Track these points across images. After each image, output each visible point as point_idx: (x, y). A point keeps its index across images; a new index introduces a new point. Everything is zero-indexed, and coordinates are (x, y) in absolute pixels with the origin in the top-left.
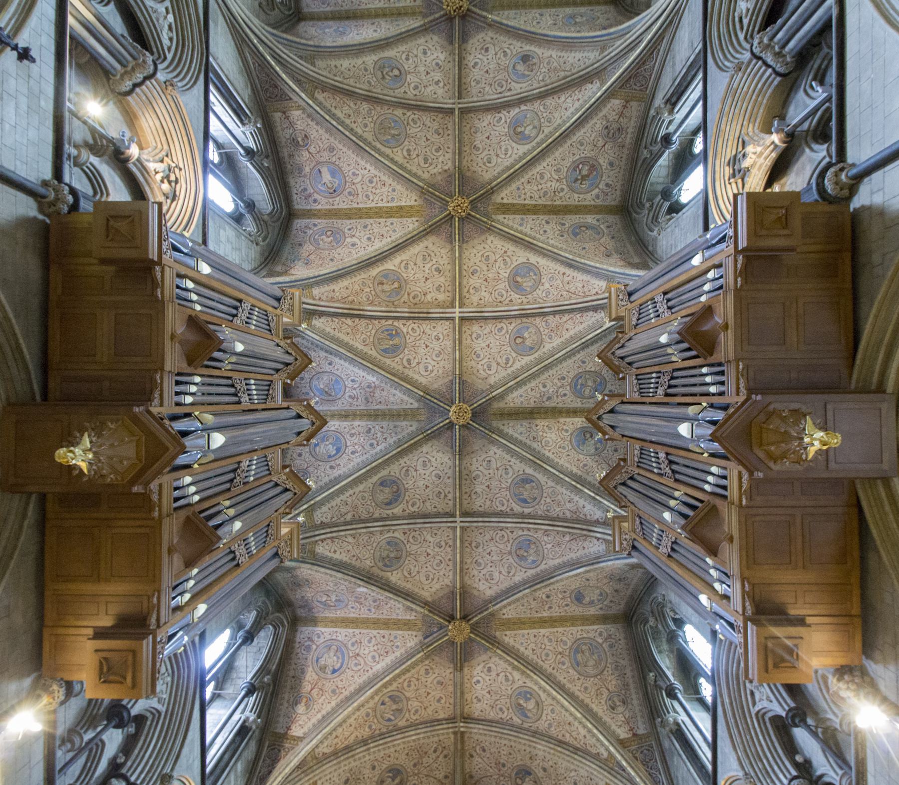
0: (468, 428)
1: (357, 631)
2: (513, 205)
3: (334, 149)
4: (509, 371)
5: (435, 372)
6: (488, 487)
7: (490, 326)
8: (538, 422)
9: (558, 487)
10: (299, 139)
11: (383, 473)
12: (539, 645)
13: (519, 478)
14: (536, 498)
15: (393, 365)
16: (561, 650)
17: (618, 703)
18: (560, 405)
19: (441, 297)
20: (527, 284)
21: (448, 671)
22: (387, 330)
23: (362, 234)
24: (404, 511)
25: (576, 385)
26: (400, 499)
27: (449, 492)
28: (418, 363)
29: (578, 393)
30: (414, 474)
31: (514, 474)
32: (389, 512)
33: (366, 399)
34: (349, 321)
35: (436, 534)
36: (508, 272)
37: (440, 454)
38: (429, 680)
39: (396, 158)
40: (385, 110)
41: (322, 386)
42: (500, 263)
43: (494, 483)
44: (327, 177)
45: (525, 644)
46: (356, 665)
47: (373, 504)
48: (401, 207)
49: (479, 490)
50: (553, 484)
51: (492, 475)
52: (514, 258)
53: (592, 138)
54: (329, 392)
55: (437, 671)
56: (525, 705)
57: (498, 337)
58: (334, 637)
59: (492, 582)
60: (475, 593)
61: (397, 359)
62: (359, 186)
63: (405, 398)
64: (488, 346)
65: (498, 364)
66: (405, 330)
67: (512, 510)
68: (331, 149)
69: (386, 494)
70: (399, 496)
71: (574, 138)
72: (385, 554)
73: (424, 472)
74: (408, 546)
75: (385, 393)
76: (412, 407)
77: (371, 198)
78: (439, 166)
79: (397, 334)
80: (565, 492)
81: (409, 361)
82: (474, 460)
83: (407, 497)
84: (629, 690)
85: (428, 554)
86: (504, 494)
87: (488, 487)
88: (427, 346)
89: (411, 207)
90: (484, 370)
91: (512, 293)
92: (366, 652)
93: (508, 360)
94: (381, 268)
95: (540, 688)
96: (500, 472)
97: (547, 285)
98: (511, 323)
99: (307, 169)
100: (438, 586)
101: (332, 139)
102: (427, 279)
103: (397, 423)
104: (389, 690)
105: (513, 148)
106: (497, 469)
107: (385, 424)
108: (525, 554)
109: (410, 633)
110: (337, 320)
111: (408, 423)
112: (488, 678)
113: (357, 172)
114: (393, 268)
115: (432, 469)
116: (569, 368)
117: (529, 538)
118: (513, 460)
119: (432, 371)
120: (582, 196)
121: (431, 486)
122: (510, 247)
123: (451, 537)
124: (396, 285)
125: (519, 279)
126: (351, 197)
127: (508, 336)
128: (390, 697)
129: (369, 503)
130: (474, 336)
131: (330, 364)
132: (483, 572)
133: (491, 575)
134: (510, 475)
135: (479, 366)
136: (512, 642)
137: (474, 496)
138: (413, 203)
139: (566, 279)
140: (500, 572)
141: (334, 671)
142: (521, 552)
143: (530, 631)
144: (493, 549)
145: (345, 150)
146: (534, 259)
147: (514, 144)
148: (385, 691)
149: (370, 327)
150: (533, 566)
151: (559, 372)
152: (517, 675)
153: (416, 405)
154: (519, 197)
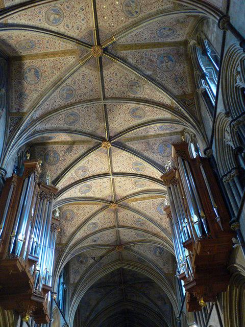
4: (87, 159)
18: (62, 146)
25: (57, 157)
29: (55, 152)
40: (141, 227)
41: (168, 149)
49: (94, 114)
55: (107, 25)
56: (55, 16)
60: (90, 68)
69: (139, 113)
86: (82, 115)
93: (88, 163)
104: (134, 19)
107: (140, 135)
117: (67, 100)
118: (80, 128)
122: (93, 196)
128: (133, 15)
133: (83, 77)
136: (68, 45)
143: (58, 50)
146: (83, 195)
153: (126, 144)
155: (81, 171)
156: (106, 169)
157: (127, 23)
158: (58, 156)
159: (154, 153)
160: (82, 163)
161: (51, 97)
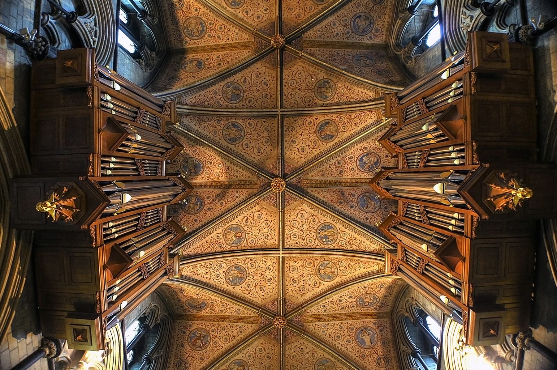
0: (273, 174)
1: (346, 40)
2: (244, 322)
3: (362, 357)
4: (245, 214)
5: (296, 213)
6: (259, 135)
7: (259, 244)
8: (226, 179)
9: (212, 136)
10: (383, 362)
11: (331, 144)
12: (226, 34)
13: (238, 142)
14: (227, 128)
15: (324, 218)
16: (212, 32)
17: (177, 4)
18: (211, 190)
19: (292, 263)
20: (234, 272)
21: (285, 16)
22: (329, 241)
23: (345, 304)
24: (317, 119)
25: (201, 205)
26: (319, 126)
27: (286, 131)
28: (308, 219)
29: (199, 199)
30: (310, 143)
31: (242, 144)
32: (326, 118)
33: (343, 194)
34: (354, 248)
35: (295, 103)
36: (247, 281)
37: (292, 157)
38: (297, 10)
39: (321, 351)
41: (373, 202)
42: (253, 286)
43: (255, 137)
44: (367, 339)
45: (235, 34)
46: (346, 20)
47: (337, 123)
48: (319, 321)
49: (265, 132)
50: (215, 138)
51: (257, 143)
52: (243, 289)
53: (195, 362)
54: (368, 199)
55: (293, 16)
57: (253, 236)
58: (361, 37)
59: (256, 72)
60: (267, 65)
61: (322, 222)
62: (346, 334)
63: (316, 195)
64: (260, 231)
65: (253, 219)
66: (317, 241)
67: (243, 120)
68: (363, 356)
69: (329, 130)
70: (320, 129)
71: (206, 362)
72: (329, 90)
73: (303, 145)
74: (313, 95)
75: (330, 198)
76: (312, 189)
77: (338, 326)
78: (293, 347)
79: (322, 238)
80: (208, 134)
81: (314, 220)
82: (269, 153)
83: (315, 128)
84: (170, 12)
85: (300, 89)
87: (259, 135)
88: (302, 230)
89: (312, 321)
90: (262, 214)
91: (244, 266)
92: (339, 28)
93: (247, 222)
94: (332, 282)
95: (225, 9)
96: (251, 145)
97: (221, 271)
98: (245, 246)
99: (379, 344)
100: (293, 69)
101: (362, 362)
102: (302, 275)
103: (322, 178)
104: (324, 5)
105: (245, 357)
106: (253, 147)
107: (330, 177)
108: (234, 91)
109: (311, 39)
110: (362, 248)
111: (314, 178)
112: (260, 12)
113: (347, 343)
114: (324, 283)
115: (298, 147)
116: (205, 216)
117: (232, 102)
118: (243, 154)
119: (298, 213)
120: (200, 326)
121: (298, 135)
122: (246, 296)
123: (284, 101)
124: (322, 272)
125: (240, 275)
126: (351, 327)
127: (247, 237)
129: (340, 124)
130: (269, 238)
131: (367, 219)
132: (263, 78)
134: (245, 143)
135: (266, 217)
136: (244, 35)
137: (269, 128)
138: (311, 324)
139: (208, 276)
140: (251, 79)
141: (360, 17)
142: (237, 92)
143: (231, 42)
144: (256, 94)
145: (355, 356)
146: (230, 288)
147: (245, 359)
148: (326, 5)
149: (340, 244)
150: (229, 84)
151: (212, 213)
152: (240, 15)
153: (309, 190)
154: (240, 327)
155: (233, 233)
156: (273, 241)
157: (315, 11)
158: (202, 204)
159: (352, 207)
160: (237, 219)
161: (212, 88)
